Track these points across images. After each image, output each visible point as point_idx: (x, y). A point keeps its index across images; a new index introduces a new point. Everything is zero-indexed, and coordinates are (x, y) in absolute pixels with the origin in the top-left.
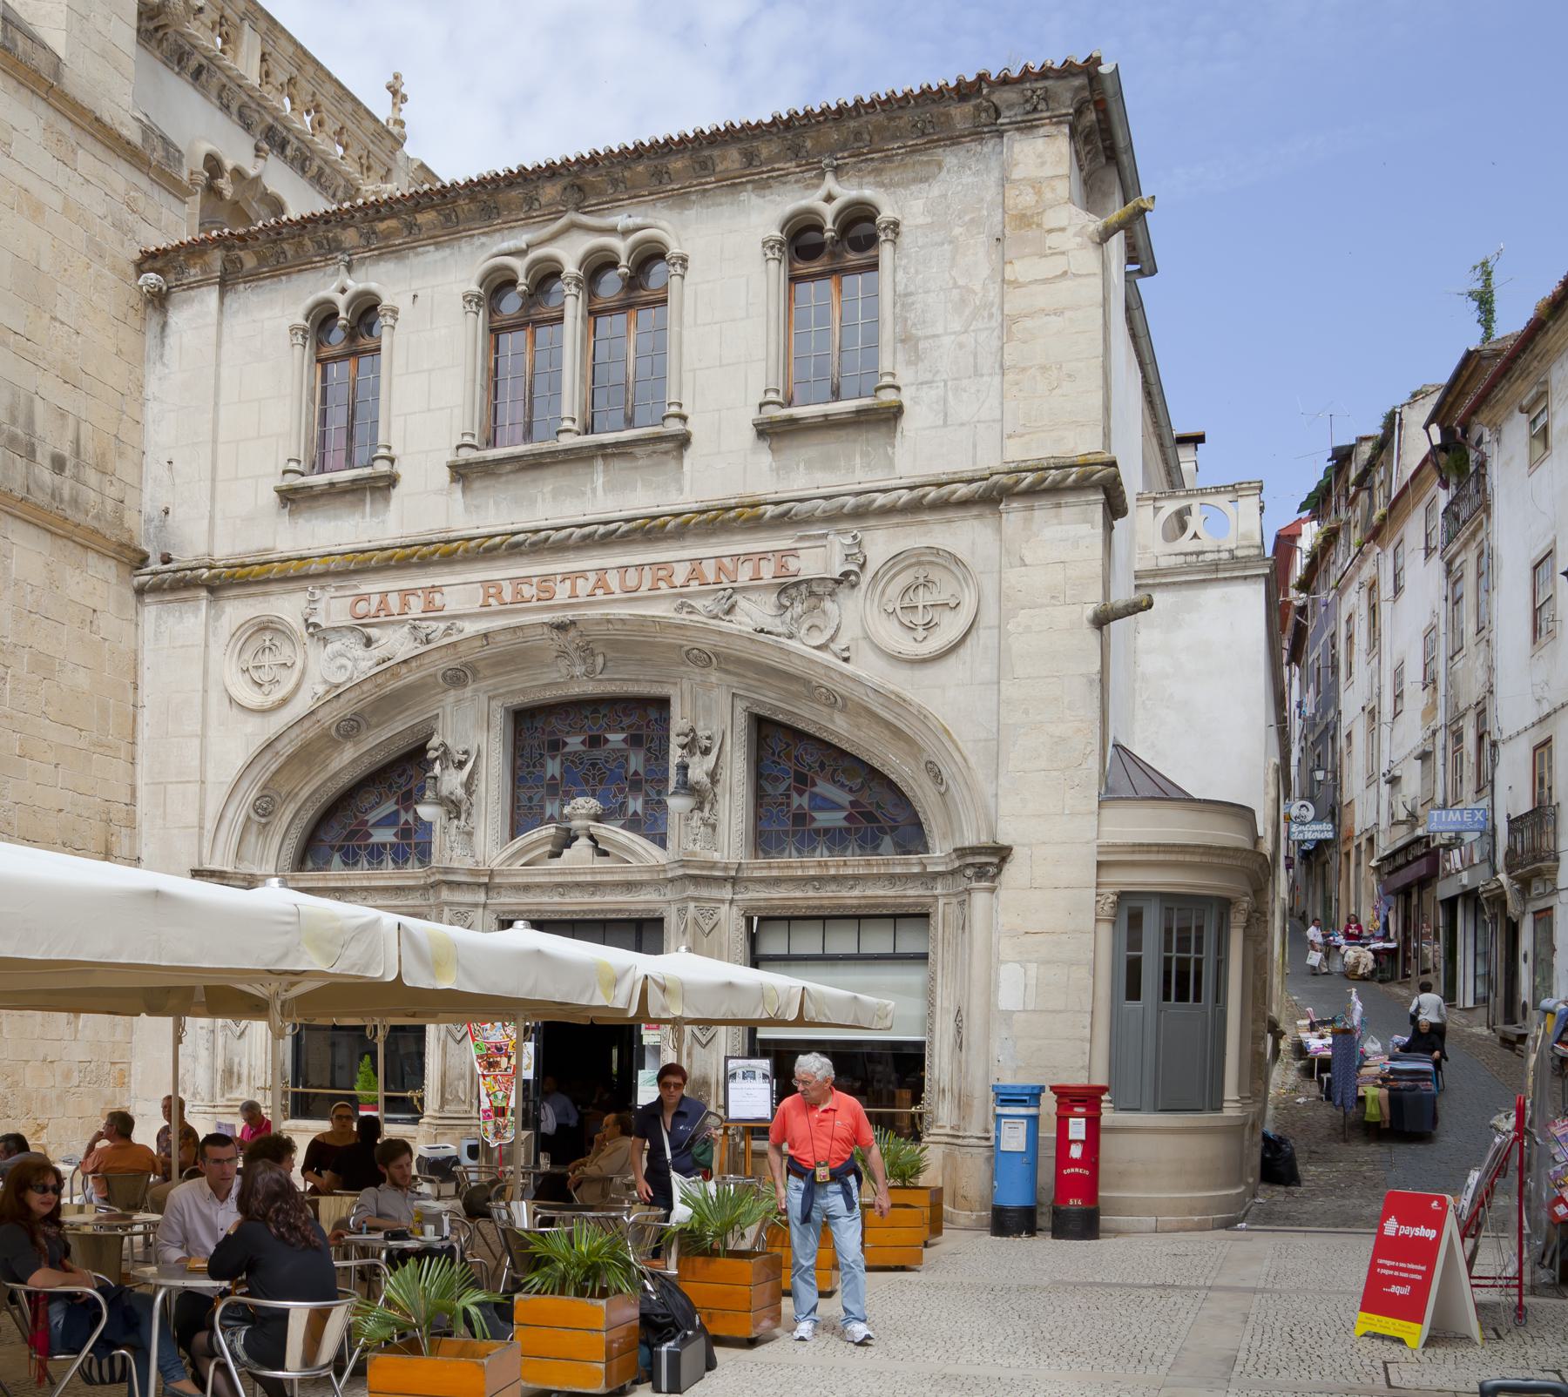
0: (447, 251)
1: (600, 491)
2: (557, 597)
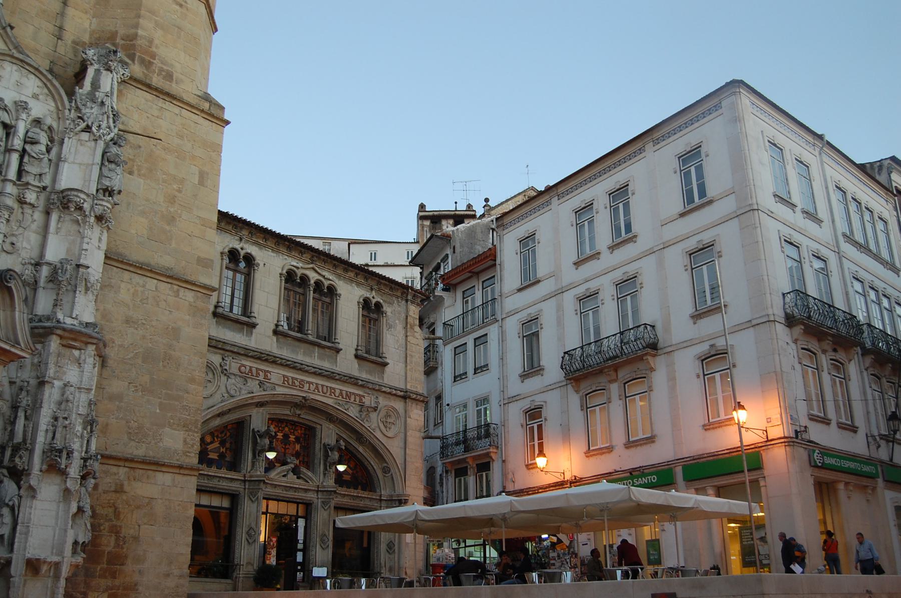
0: (275, 255)
1: (316, 357)
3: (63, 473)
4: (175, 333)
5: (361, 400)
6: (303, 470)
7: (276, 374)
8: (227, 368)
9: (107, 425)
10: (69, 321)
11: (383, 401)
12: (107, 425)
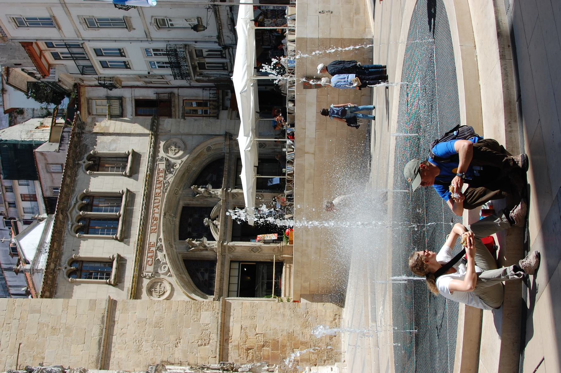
0: (65, 242)
2: (157, 216)
5: (162, 172)
6: (212, 214)
7: (152, 238)
8: (150, 274)
9: (201, 358)
12: (201, 358)
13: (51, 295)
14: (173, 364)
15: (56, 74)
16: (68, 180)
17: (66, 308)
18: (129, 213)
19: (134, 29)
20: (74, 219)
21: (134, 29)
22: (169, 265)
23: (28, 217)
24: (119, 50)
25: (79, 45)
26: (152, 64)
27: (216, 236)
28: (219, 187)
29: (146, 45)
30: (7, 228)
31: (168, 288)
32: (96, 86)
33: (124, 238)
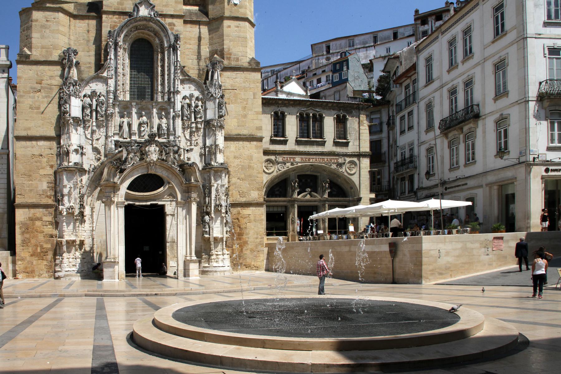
3: (221, 211)
4: (251, 158)
10: (216, 164)
11: (348, 159)
13: (263, 104)
14: (229, 177)
15: (397, 89)
16: (330, 105)
17: (257, 113)
18: (312, 143)
19: (426, 134)
20: (307, 112)
21: (426, 134)
22: (283, 170)
23: (308, 84)
24: (412, 126)
25: (415, 100)
26: (402, 149)
27: (300, 197)
28: (329, 196)
29: (416, 143)
30: (301, 72)
31: (270, 171)
32: (389, 114)
33: (298, 143)
